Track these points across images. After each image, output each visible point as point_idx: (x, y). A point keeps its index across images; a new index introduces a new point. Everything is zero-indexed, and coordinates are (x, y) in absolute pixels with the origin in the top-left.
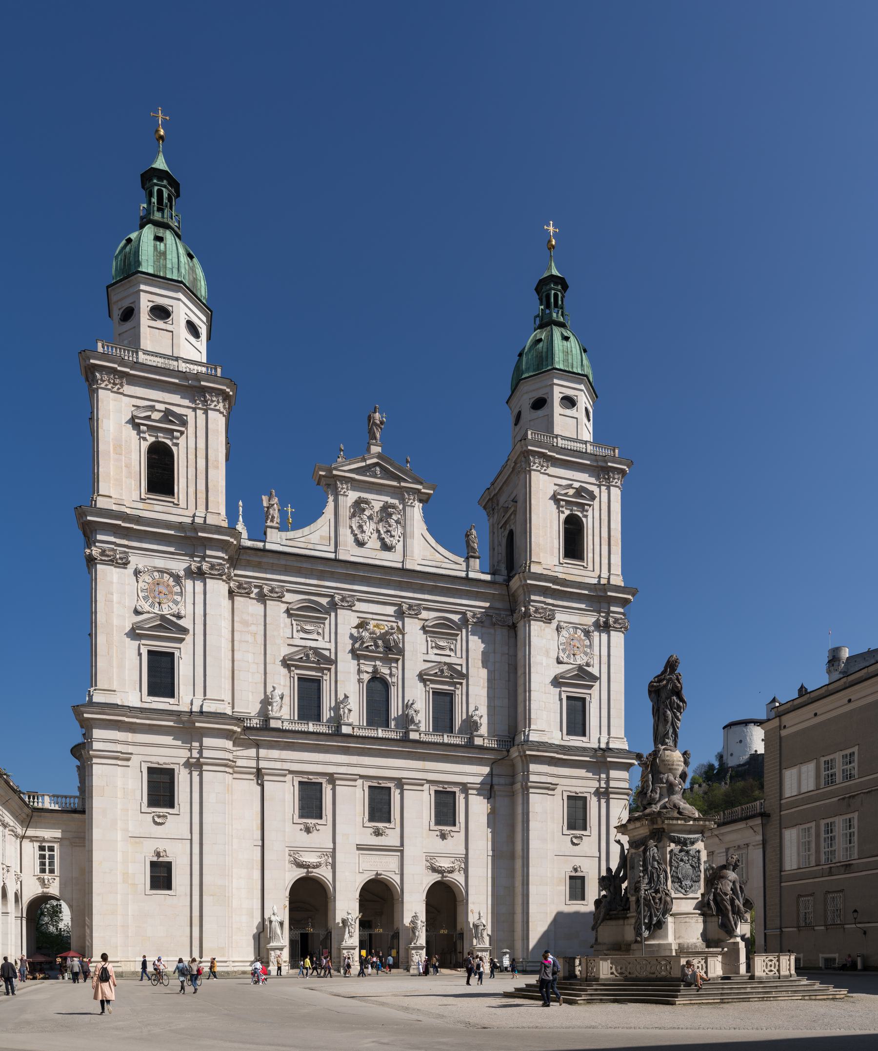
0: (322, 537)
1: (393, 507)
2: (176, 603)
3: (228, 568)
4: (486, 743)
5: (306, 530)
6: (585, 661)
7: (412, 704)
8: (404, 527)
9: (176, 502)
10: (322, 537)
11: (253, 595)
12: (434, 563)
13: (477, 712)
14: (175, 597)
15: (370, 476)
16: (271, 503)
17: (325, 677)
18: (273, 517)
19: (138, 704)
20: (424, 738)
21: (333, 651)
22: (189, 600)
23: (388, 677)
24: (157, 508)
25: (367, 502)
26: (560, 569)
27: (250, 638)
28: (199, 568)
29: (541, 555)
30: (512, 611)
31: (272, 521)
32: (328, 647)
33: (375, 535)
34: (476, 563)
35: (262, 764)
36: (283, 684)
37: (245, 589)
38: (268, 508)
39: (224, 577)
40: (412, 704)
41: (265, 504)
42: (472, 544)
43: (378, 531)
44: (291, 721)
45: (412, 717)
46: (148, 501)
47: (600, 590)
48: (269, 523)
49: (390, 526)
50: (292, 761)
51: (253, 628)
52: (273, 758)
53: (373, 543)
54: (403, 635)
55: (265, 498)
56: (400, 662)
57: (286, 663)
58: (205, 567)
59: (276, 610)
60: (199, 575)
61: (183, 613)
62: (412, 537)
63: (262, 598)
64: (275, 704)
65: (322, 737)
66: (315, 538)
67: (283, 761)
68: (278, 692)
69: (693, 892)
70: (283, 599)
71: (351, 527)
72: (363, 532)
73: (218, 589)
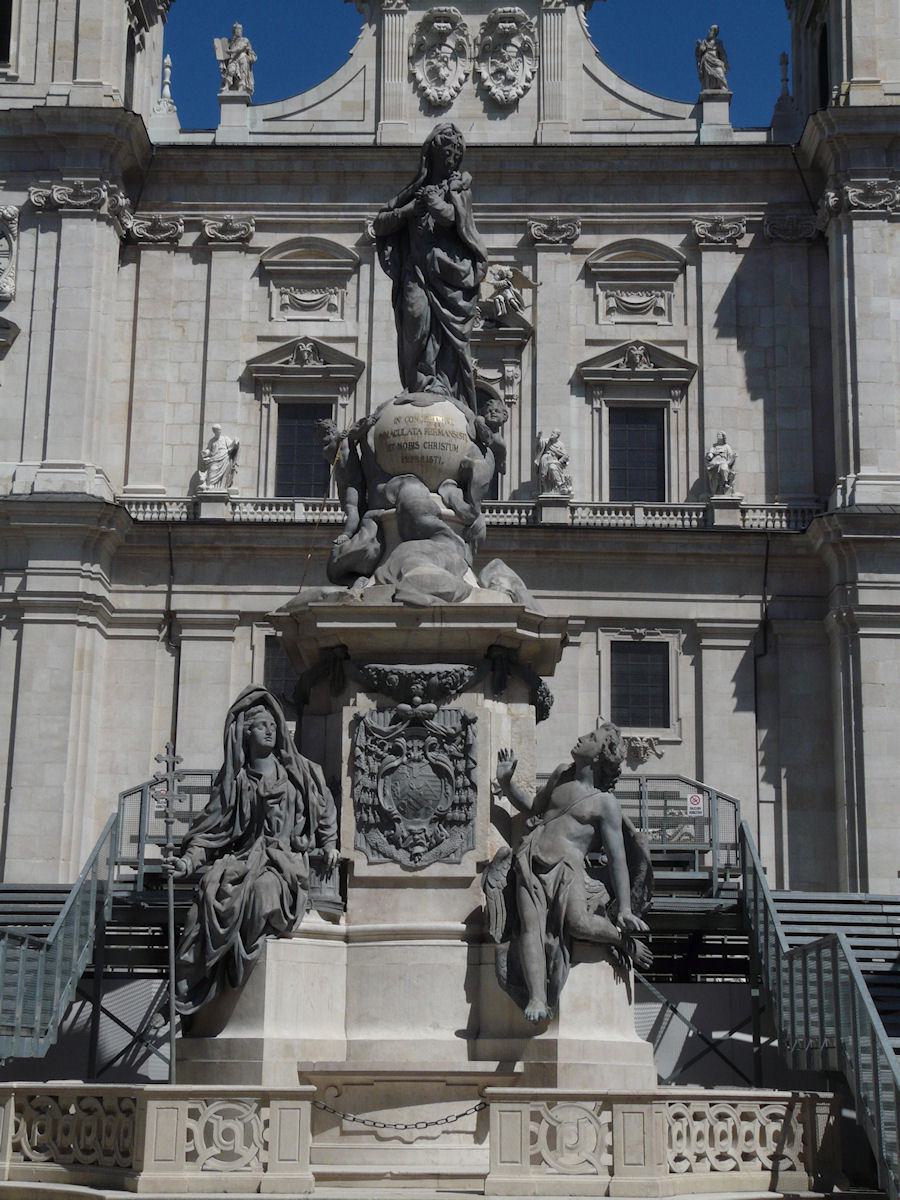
1: (512, 19)
3: (111, 192)
4: (757, 520)
5: (311, 96)
7: (552, 441)
8: (539, 58)
9: (11, 72)
11: (182, 243)
13: (722, 449)
16: (236, 54)
17: (341, 400)
18: (236, 79)
20: (583, 517)
21: (363, 339)
22: (26, 263)
23: (496, 387)
27: (171, 332)
28: (49, 199)
29: (881, 64)
30: (813, 202)
31: (234, 87)
32: (351, 333)
33: (470, 86)
34: (717, 113)
35: (180, 602)
36: (247, 430)
38: (226, 62)
39: (104, 210)
40: (552, 441)
41: (220, 55)
42: (710, 71)
43: (477, 75)
44: (262, 505)
45: (550, 471)
48: (226, 92)
49: (505, 61)
51: (183, 311)
54: (535, 289)
55: (220, 47)
56: (526, 355)
57: (254, 381)
58: (59, 193)
59: (235, 270)
62: (559, 74)
63: (202, 252)
64: (214, 467)
66: (327, 110)
68: (225, 442)
69: (444, 858)
70: (251, 244)
71: (412, 76)
72: (441, 81)
73: (91, 241)
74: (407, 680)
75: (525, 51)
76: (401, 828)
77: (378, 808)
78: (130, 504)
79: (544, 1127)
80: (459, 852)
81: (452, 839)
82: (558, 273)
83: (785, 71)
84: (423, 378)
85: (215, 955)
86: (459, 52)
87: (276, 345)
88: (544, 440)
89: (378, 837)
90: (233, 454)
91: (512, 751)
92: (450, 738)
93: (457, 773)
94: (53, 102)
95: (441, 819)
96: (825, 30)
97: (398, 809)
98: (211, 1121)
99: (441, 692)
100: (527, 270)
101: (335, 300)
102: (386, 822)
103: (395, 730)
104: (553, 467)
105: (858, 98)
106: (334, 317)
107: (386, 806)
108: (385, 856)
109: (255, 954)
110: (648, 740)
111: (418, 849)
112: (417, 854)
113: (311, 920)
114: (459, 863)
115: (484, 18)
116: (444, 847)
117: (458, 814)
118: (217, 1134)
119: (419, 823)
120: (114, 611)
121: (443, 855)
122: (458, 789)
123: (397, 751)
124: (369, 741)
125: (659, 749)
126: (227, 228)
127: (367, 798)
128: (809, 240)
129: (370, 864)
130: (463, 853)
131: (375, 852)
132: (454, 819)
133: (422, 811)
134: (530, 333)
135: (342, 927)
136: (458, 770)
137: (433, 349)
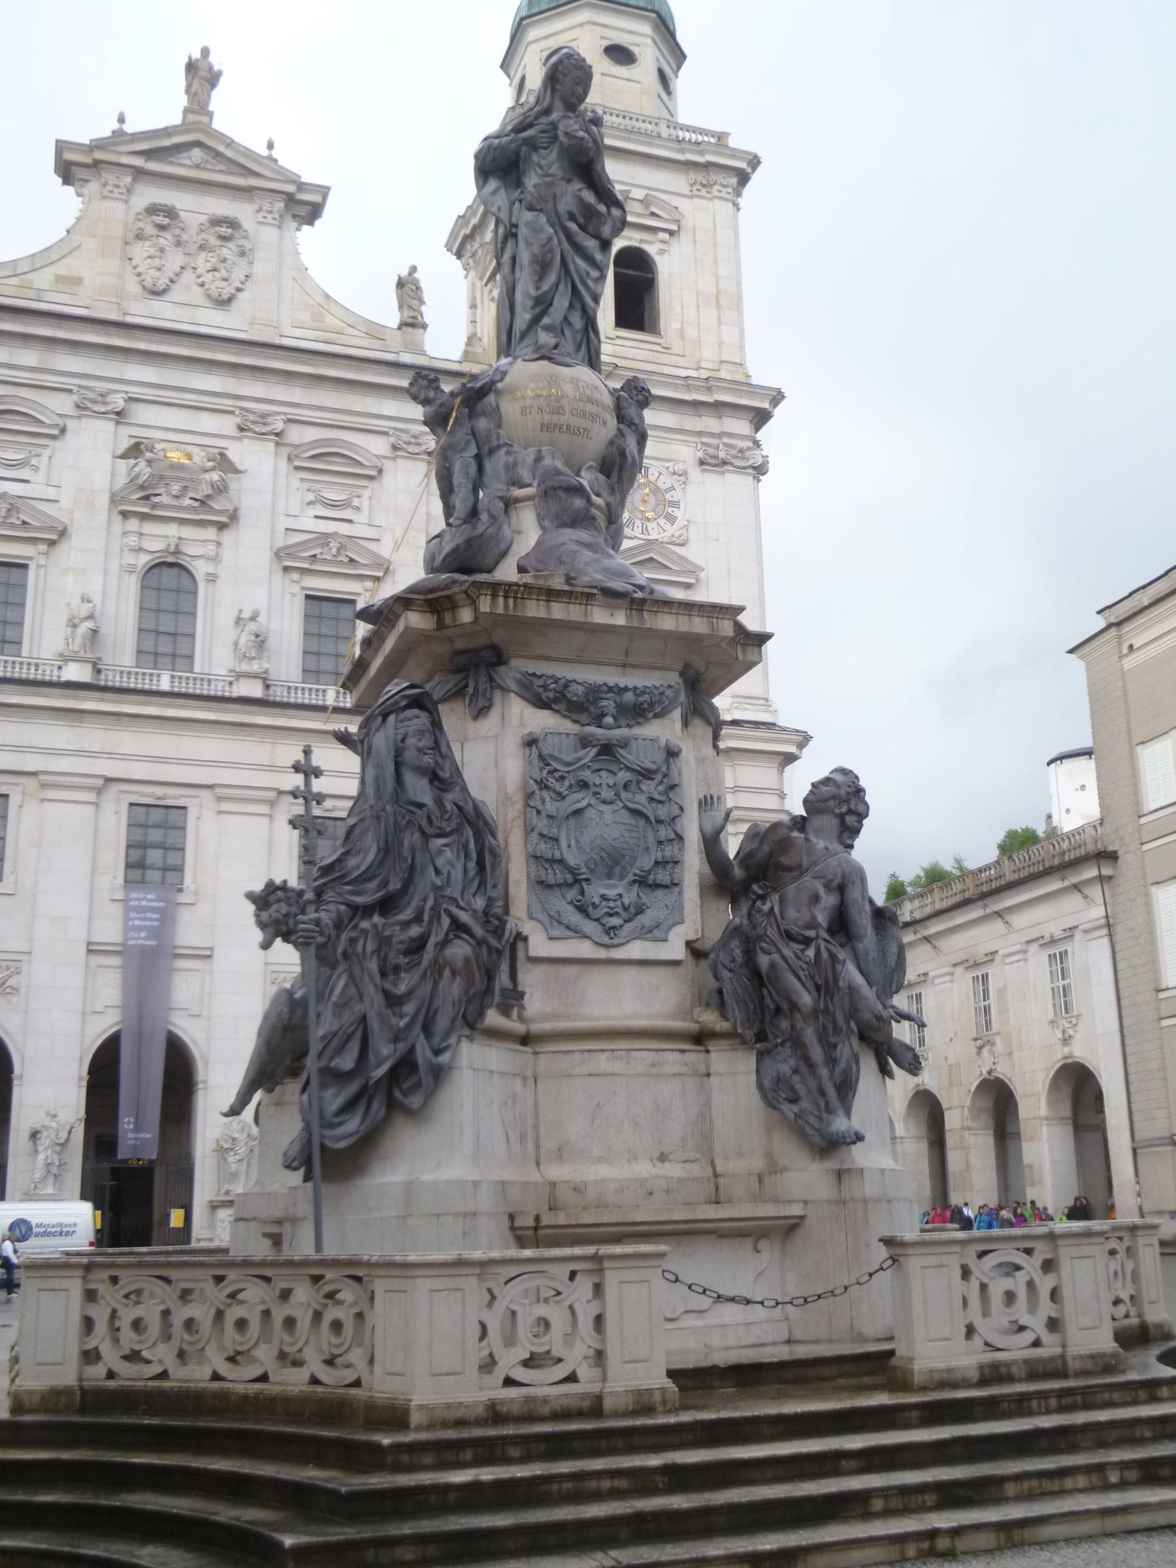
1: (233, 224)
74: (595, 693)
75: (242, 254)
76: (594, 891)
77: (561, 861)
79: (975, 1285)
80: (664, 927)
81: (657, 905)
82: (257, 461)
84: (545, 338)
85: (385, 1053)
86: (178, 244)
89: (561, 903)
91: (719, 798)
92: (646, 774)
93: (660, 822)
95: (642, 881)
97: (588, 868)
98: (514, 1307)
99: (639, 710)
100: (232, 455)
101: (34, 461)
102: (577, 880)
103: (580, 759)
106: (39, 478)
107: (572, 861)
108: (568, 927)
109: (444, 1058)
111: (615, 921)
112: (613, 928)
113: (493, 1018)
114: (665, 940)
115: (203, 219)
116: (646, 919)
117: (662, 876)
118: (524, 1325)
119: (614, 886)
121: (645, 930)
122: (660, 843)
123: (584, 785)
124: (545, 772)
127: (544, 848)
129: (551, 938)
130: (670, 928)
131: (555, 924)
132: (656, 880)
133: (617, 870)
134: (234, 516)
135: (518, 1027)
136: (657, 819)
137: (561, 302)
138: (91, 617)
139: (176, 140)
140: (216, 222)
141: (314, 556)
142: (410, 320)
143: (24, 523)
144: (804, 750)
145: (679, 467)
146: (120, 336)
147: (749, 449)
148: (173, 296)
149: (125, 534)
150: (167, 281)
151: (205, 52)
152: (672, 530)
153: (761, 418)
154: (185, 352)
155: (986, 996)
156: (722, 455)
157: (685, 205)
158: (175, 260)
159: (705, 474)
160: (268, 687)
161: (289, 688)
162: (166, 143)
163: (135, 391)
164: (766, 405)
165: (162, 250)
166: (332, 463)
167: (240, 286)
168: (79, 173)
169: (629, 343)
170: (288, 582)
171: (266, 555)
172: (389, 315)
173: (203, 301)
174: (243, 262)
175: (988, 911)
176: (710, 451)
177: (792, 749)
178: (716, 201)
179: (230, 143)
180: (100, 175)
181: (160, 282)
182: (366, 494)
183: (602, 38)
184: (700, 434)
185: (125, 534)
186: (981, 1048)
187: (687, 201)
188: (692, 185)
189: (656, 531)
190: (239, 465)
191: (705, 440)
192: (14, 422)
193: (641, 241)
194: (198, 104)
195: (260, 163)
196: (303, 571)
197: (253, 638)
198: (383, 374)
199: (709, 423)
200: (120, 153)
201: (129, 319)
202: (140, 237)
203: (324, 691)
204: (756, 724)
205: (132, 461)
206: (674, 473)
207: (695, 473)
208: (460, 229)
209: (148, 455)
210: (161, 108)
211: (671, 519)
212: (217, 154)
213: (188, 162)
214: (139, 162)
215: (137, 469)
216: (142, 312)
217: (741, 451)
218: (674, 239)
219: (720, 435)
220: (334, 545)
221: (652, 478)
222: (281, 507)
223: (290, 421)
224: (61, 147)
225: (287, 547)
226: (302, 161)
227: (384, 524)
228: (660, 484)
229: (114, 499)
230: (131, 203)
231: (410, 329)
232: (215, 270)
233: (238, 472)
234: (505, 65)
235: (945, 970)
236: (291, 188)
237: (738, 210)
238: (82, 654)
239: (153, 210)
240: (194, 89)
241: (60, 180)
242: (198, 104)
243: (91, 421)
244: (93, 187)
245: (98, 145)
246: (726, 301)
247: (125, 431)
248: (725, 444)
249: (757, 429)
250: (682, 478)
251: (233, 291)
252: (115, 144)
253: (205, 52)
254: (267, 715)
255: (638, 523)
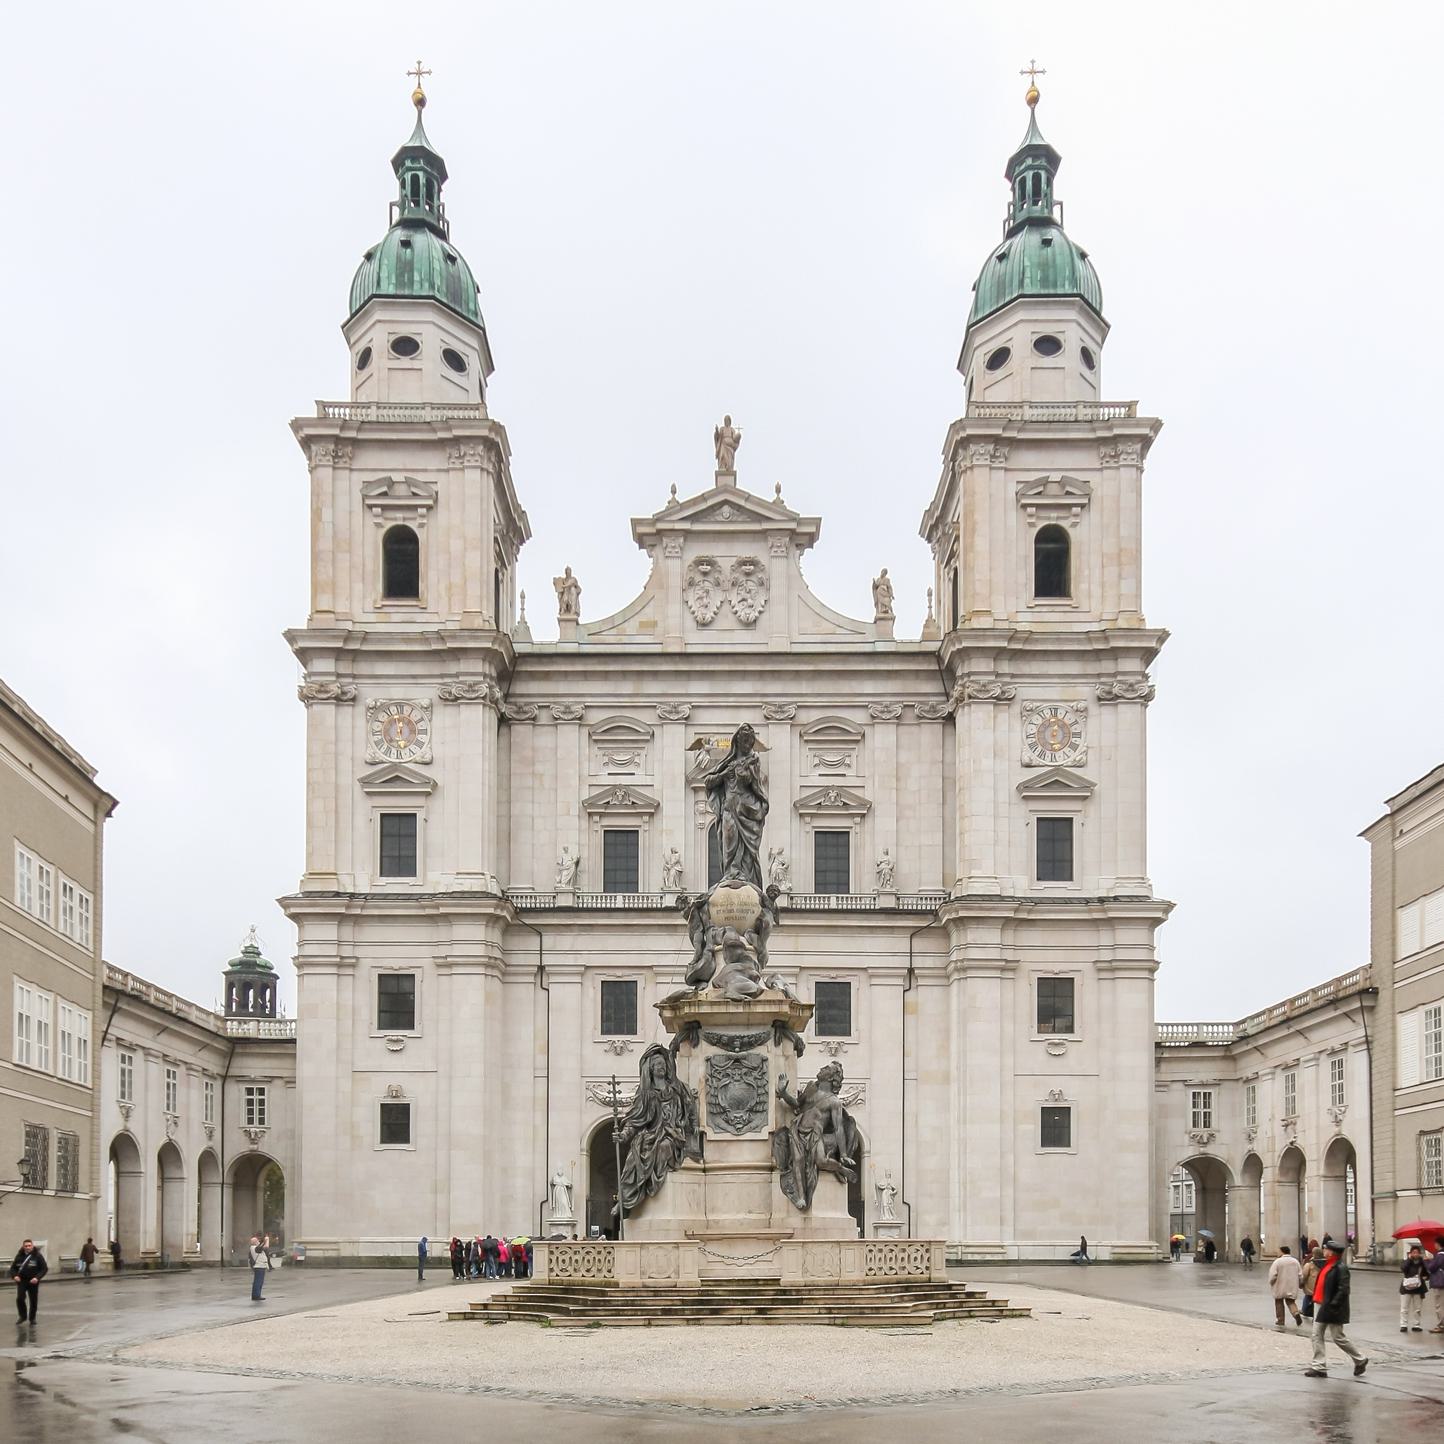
0: (642, 624)
1: (753, 562)
2: (420, 744)
3: (490, 687)
6: (1071, 759)
10: (642, 624)
12: (819, 638)
14: (419, 737)
15: (713, 522)
19: (364, 889)
24: (396, 618)
25: (710, 562)
26: (1029, 617)
35: (547, 960)
36: (584, 844)
37: (526, 713)
46: (386, 610)
47: (1097, 640)
50: (590, 952)
52: (564, 948)
53: (726, 621)
60: (451, 700)
61: (427, 759)
64: (565, 873)
65: (633, 914)
67: (577, 952)
78: (513, 897)
83: (930, 603)
86: (718, 584)
87: (601, 790)
88: (775, 852)
90: (577, 863)
94: (451, 626)
96: (956, 570)
104: (779, 871)
105: (976, 623)
110: (838, 1043)
120: (506, 965)
125: (845, 1048)
126: (568, 710)
128: (944, 718)
138: (678, 862)
139: (710, 502)
140: (744, 563)
141: (820, 804)
142: (883, 615)
143: (633, 803)
144: (1170, 915)
145: (1082, 705)
146: (685, 663)
147: (1139, 682)
148: (717, 625)
149: (696, 803)
150: (712, 614)
151: (728, 421)
152: (1075, 756)
153: (1149, 655)
154: (726, 668)
155: (1294, 1090)
156: (1116, 690)
157: (1094, 479)
158: (717, 597)
159: (1103, 707)
160: (792, 898)
161: (806, 898)
162: (703, 506)
163: (696, 701)
164: (1153, 644)
165: (707, 592)
166: (829, 735)
167: (761, 609)
168: (648, 541)
169: (1045, 609)
170: (803, 824)
171: (788, 806)
172: (867, 613)
173: (736, 625)
174: (762, 591)
175: (1292, 1030)
176: (1107, 688)
177: (1159, 915)
178: (1122, 469)
179: (748, 498)
180: (662, 540)
181: (708, 616)
182: (854, 754)
183: (1033, 333)
184: (1099, 675)
185: (696, 803)
186: (1287, 1126)
187: (1098, 474)
188: (1102, 459)
189: (1062, 758)
190: (765, 745)
191: (1103, 680)
192: (623, 734)
193: (1058, 518)
194: (726, 470)
195: (770, 509)
196: (812, 816)
197: (781, 867)
198: (862, 663)
199: (1107, 666)
200: (673, 521)
201: (690, 649)
202: (691, 584)
203: (829, 898)
204: (1131, 898)
205: (698, 752)
206: (1077, 711)
207: (1094, 709)
208: (928, 521)
209: (707, 746)
210: (698, 480)
211: (1074, 747)
212: (739, 508)
213: (720, 518)
214: (686, 526)
215: (700, 757)
216: (699, 641)
217: (1131, 685)
218: (1085, 513)
219: (1114, 675)
220: (833, 794)
221: (1060, 717)
222: (797, 772)
223: (799, 707)
224: (635, 523)
225: (801, 800)
226: (799, 504)
227: (867, 775)
228: (1066, 720)
229: (688, 782)
230: (684, 557)
231: (883, 622)
232: (744, 600)
233: (766, 750)
234: (959, 367)
235: (1268, 1071)
236: (793, 525)
237: (1142, 472)
238: (674, 888)
239: (699, 562)
240: (721, 455)
241: (637, 545)
242: (726, 470)
243: (669, 726)
244: (658, 551)
245: (658, 518)
246: (1128, 558)
247: (692, 730)
248: (1120, 682)
249: (1148, 664)
250: (1084, 714)
251: (757, 614)
252: (670, 514)
253: (728, 421)
254: (792, 919)
255: (1048, 753)
